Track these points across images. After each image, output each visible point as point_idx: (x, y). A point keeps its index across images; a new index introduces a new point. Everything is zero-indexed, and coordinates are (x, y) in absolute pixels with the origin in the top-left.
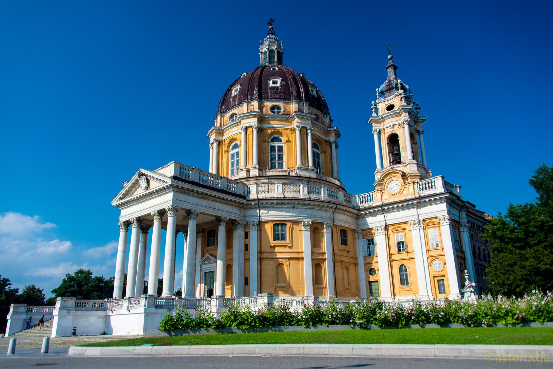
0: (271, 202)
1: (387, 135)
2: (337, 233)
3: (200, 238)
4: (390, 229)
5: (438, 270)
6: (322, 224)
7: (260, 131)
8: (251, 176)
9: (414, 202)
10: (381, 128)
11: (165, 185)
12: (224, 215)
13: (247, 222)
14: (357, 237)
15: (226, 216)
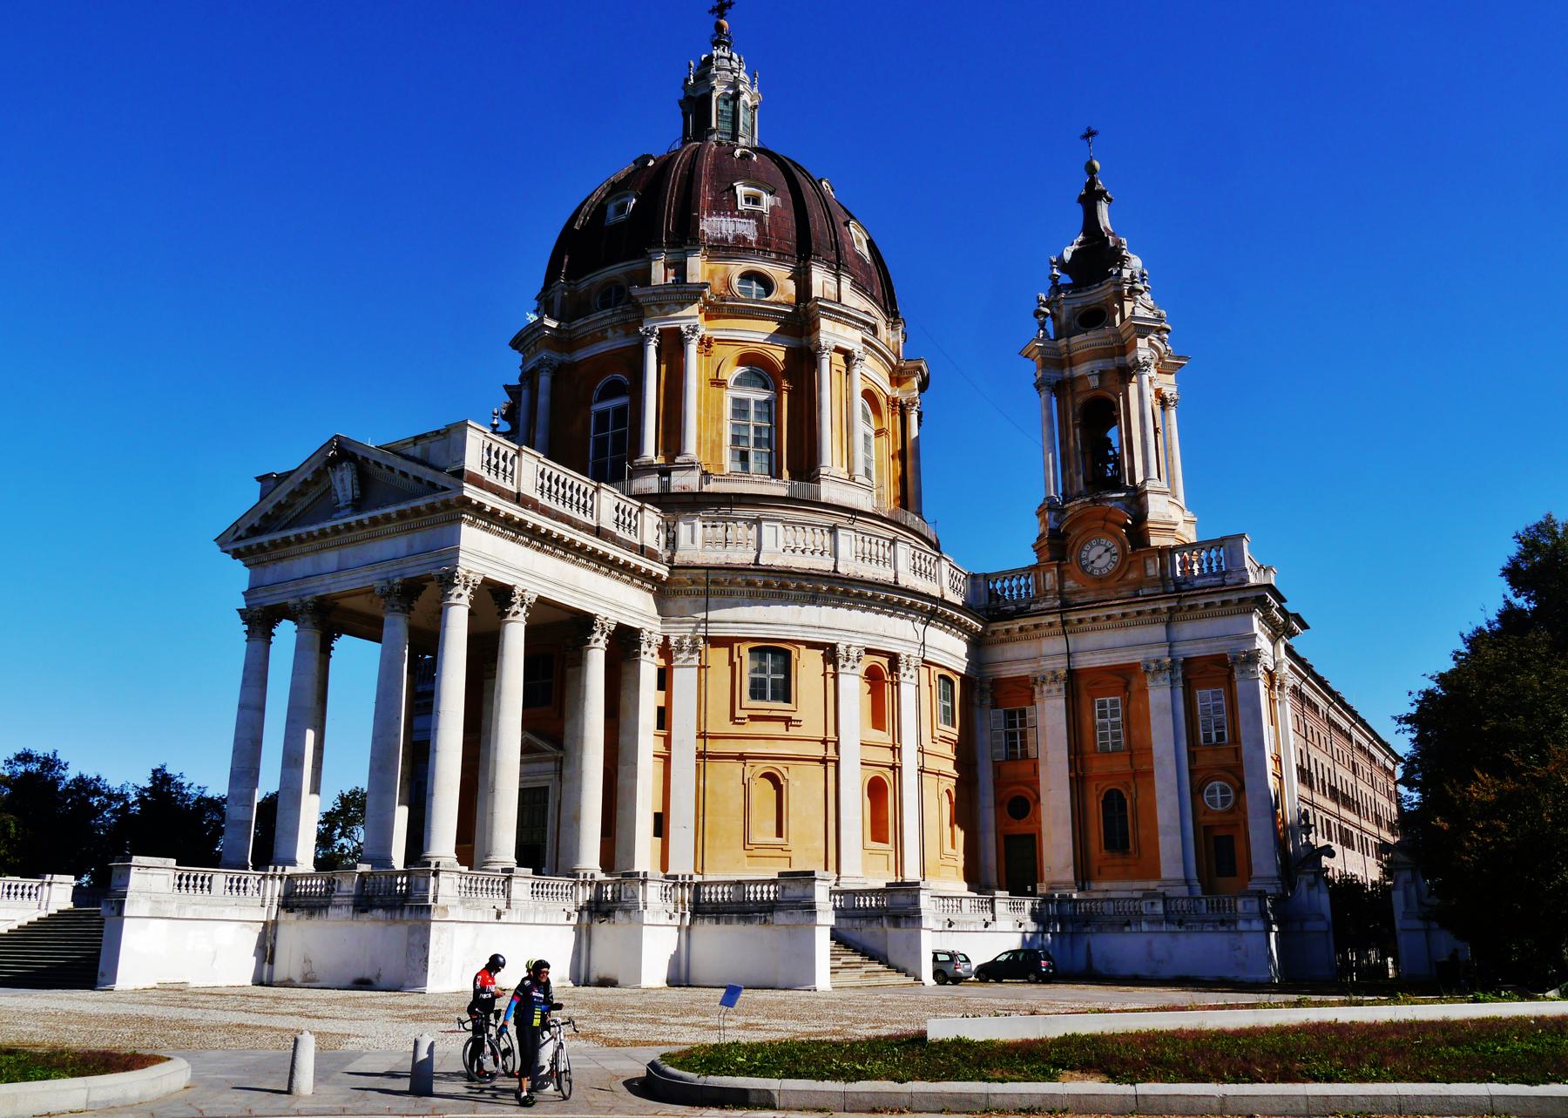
0: (749, 578)
1: (1079, 400)
2: (930, 686)
4: (1083, 683)
5: (1219, 809)
6: (894, 659)
7: (706, 344)
8: (672, 491)
9: (1163, 606)
13: (666, 638)
14: (977, 701)
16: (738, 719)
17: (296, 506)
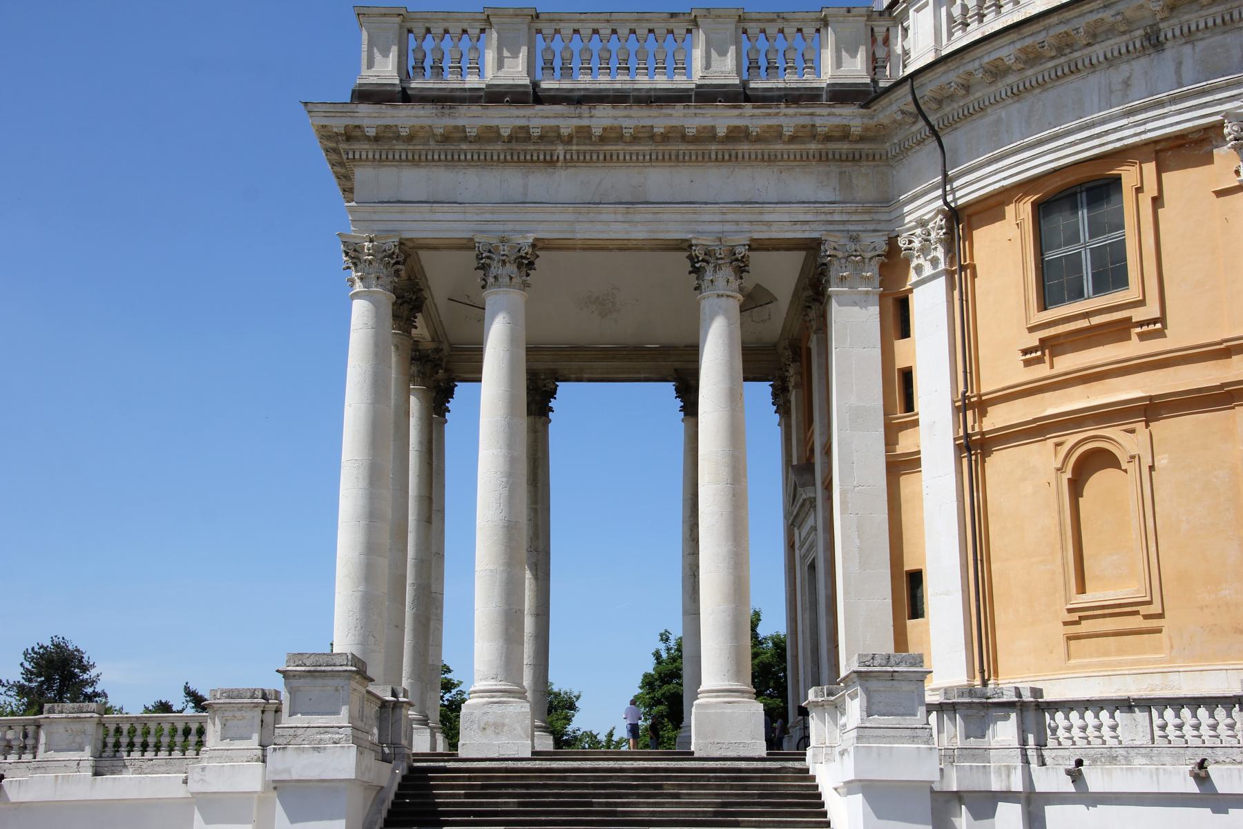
0: (986, 59)
12: (718, 227)
15: (727, 227)
16: (1025, 352)
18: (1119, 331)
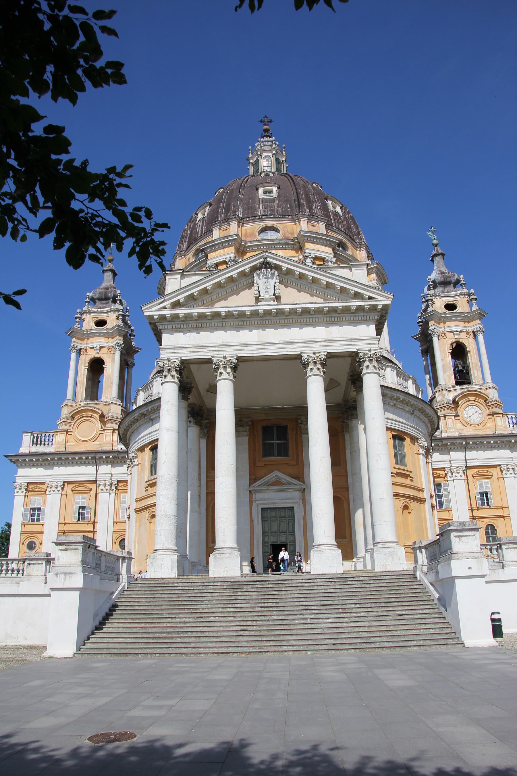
3: (246, 436)
10: (442, 330)
11: (367, 304)
17: (213, 294)
18: (406, 476)
